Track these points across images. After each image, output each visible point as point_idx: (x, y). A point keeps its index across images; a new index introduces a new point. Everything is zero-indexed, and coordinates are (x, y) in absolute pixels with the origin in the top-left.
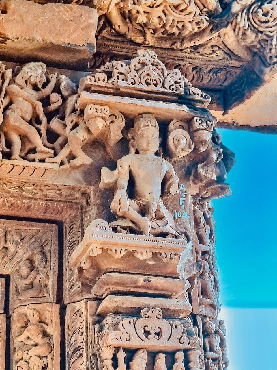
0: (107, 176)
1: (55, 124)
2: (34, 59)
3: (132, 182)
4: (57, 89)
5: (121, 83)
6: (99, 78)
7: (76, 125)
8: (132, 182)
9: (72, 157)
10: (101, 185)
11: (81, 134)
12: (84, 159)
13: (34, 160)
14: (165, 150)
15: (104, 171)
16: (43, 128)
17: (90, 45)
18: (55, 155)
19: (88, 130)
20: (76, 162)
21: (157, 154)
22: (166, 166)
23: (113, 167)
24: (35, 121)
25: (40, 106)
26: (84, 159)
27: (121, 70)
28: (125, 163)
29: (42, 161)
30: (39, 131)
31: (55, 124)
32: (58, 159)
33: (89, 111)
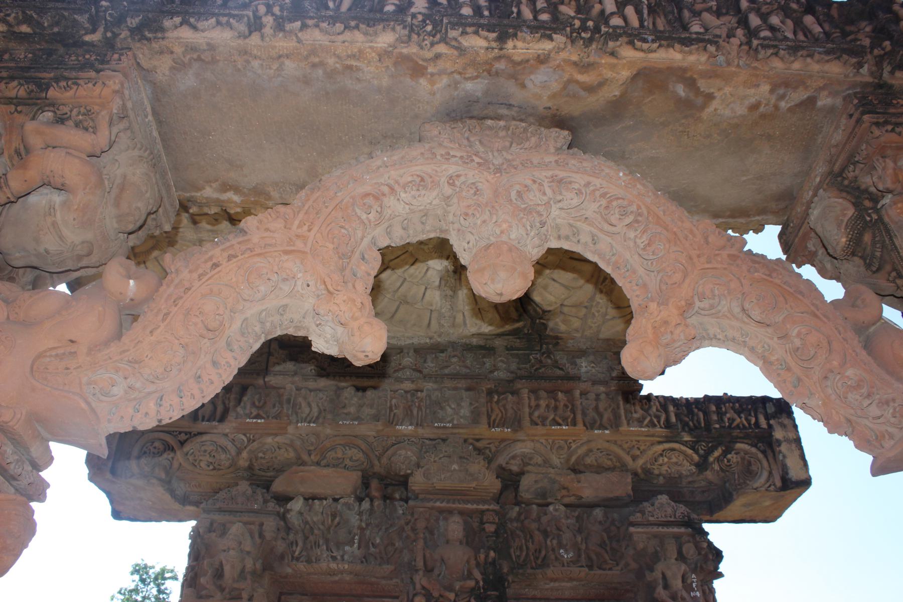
0: (649, 577)
2: (599, 506)
3: (664, 577)
5: (651, 519)
7: (628, 546)
13: (604, 570)
14: (681, 557)
15: (647, 573)
16: (608, 548)
17: (629, 496)
18: (617, 565)
19: (635, 549)
21: (676, 559)
22: (683, 567)
23: (652, 570)
24: (602, 545)
25: (605, 535)
26: (634, 565)
27: (650, 509)
28: (660, 567)
29: (610, 569)
30: (606, 550)
32: (619, 568)
33: (635, 538)
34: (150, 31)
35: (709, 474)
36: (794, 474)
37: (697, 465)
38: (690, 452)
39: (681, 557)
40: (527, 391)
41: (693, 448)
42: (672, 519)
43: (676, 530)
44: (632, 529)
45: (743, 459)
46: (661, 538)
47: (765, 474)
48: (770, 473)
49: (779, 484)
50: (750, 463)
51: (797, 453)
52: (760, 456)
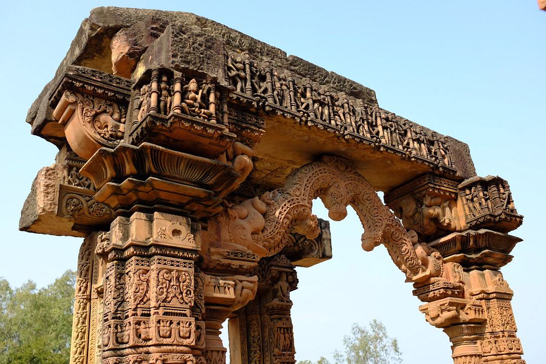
0: (276, 287)
1: (264, 273)
4: (263, 263)
6: (274, 263)
8: (281, 288)
9: (267, 281)
10: (274, 288)
11: (270, 276)
12: (270, 282)
20: (268, 283)
28: (280, 283)
31: (264, 273)
33: (273, 271)
34: (272, 114)
35: (296, 248)
36: (327, 253)
37: (294, 243)
38: (293, 238)
39: (287, 281)
40: (238, 201)
41: (294, 236)
42: (286, 265)
43: (287, 270)
44: (273, 268)
45: (310, 243)
46: (280, 273)
47: (317, 251)
48: (319, 250)
49: (321, 256)
50: (312, 246)
51: (329, 244)
52: (316, 243)
